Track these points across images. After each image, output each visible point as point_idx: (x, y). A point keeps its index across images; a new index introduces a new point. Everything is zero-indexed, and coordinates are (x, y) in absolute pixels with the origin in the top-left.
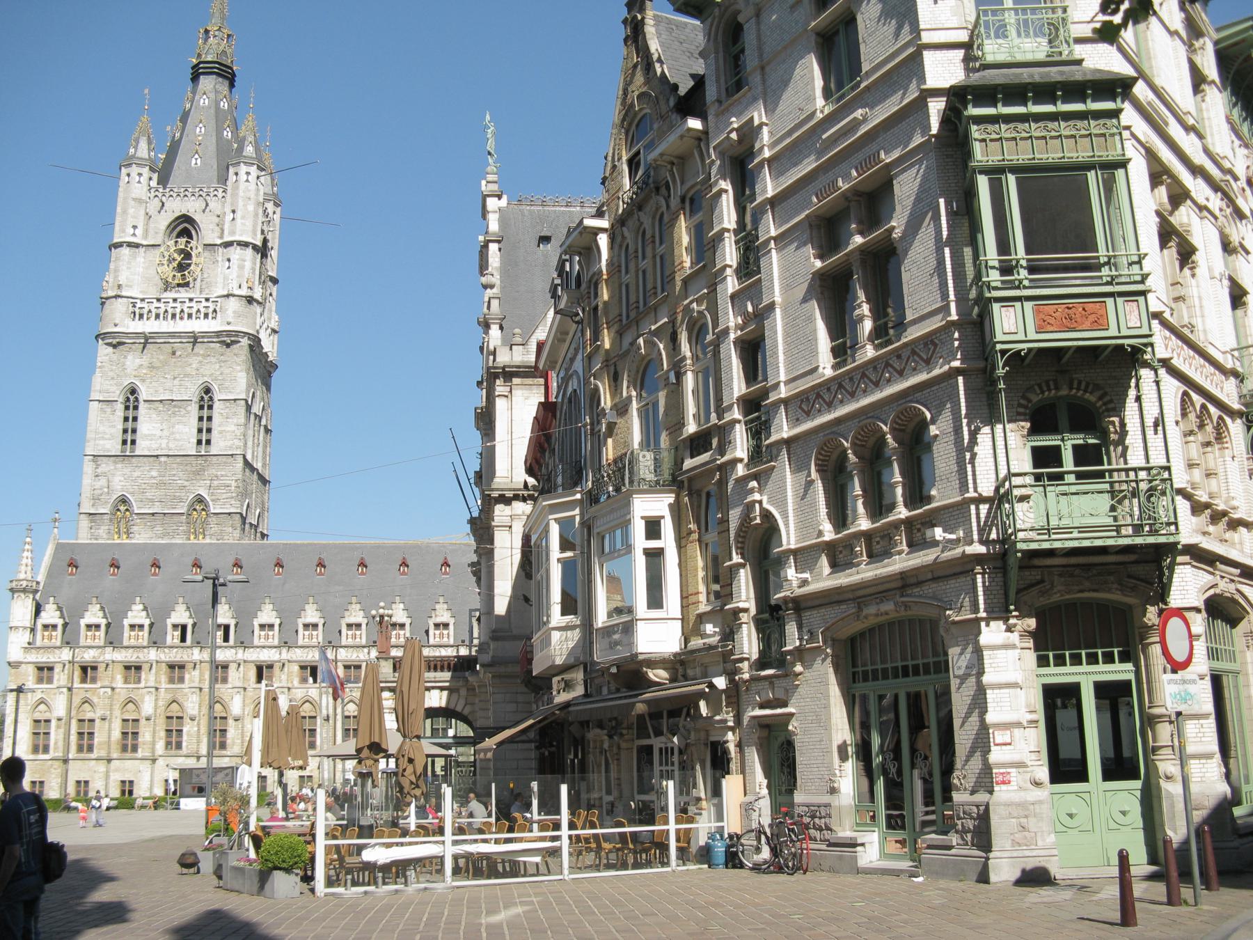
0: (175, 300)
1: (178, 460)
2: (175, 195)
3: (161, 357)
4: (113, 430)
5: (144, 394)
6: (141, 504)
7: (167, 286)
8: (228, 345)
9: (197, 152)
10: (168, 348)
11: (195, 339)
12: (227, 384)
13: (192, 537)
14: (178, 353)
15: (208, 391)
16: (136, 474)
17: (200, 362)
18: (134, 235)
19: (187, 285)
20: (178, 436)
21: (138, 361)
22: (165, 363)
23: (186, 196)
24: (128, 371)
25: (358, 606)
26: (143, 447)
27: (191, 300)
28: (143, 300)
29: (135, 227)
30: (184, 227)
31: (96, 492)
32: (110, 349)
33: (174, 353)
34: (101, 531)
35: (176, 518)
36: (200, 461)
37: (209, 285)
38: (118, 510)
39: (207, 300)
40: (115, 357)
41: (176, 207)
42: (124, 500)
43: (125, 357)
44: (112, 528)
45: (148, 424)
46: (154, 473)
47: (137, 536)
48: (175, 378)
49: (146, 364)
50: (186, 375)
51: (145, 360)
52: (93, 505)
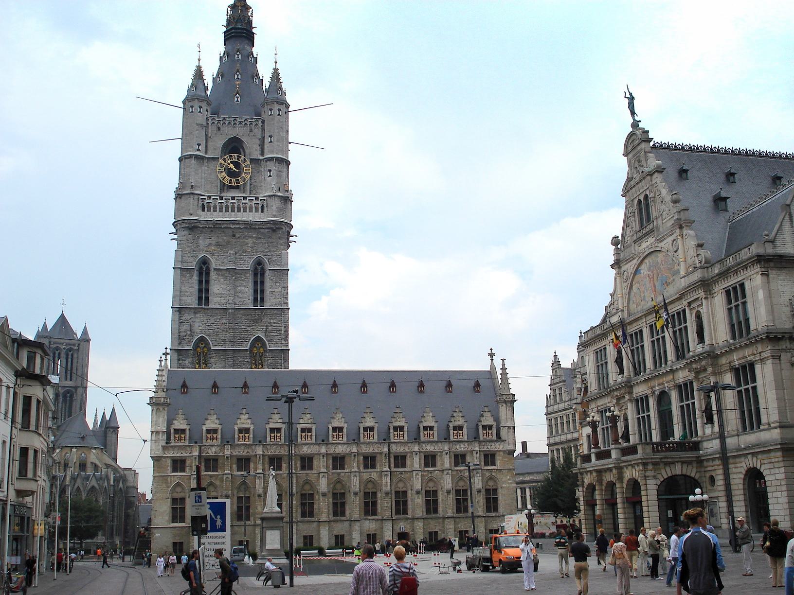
0: (233, 198)
1: (242, 312)
2: (227, 123)
3: (225, 238)
4: (192, 290)
5: (214, 264)
6: (215, 343)
7: (224, 187)
8: (274, 231)
9: (238, 93)
10: (230, 232)
11: (250, 226)
12: (274, 258)
13: (254, 366)
14: (237, 236)
15: (259, 263)
16: (210, 322)
17: (254, 242)
18: (199, 150)
19: (237, 188)
20: (240, 295)
21: (208, 241)
22: (228, 243)
23: (235, 124)
24: (201, 247)
25: (183, 416)
26: (215, 301)
27: (245, 198)
28: (210, 197)
29: (199, 145)
30: (234, 146)
31: (182, 334)
32: (186, 232)
33: (234, 236)
34: (187, 362)
35: (242, 354)
36: (258, 312)
37: (256, 187)
38: (199, 347)
39: (257, 198)
40: (190, 237)
41: (230, 132)
42: (202, 340)
43: (198, 238)
44: (194, 359)
45: (218, 288)
46: (224, 321)
47: (214, 366)
48: (236, 253)
49: (213, 243)
50: (245, 252)
51: (214, 239)
52: (180, 344)
